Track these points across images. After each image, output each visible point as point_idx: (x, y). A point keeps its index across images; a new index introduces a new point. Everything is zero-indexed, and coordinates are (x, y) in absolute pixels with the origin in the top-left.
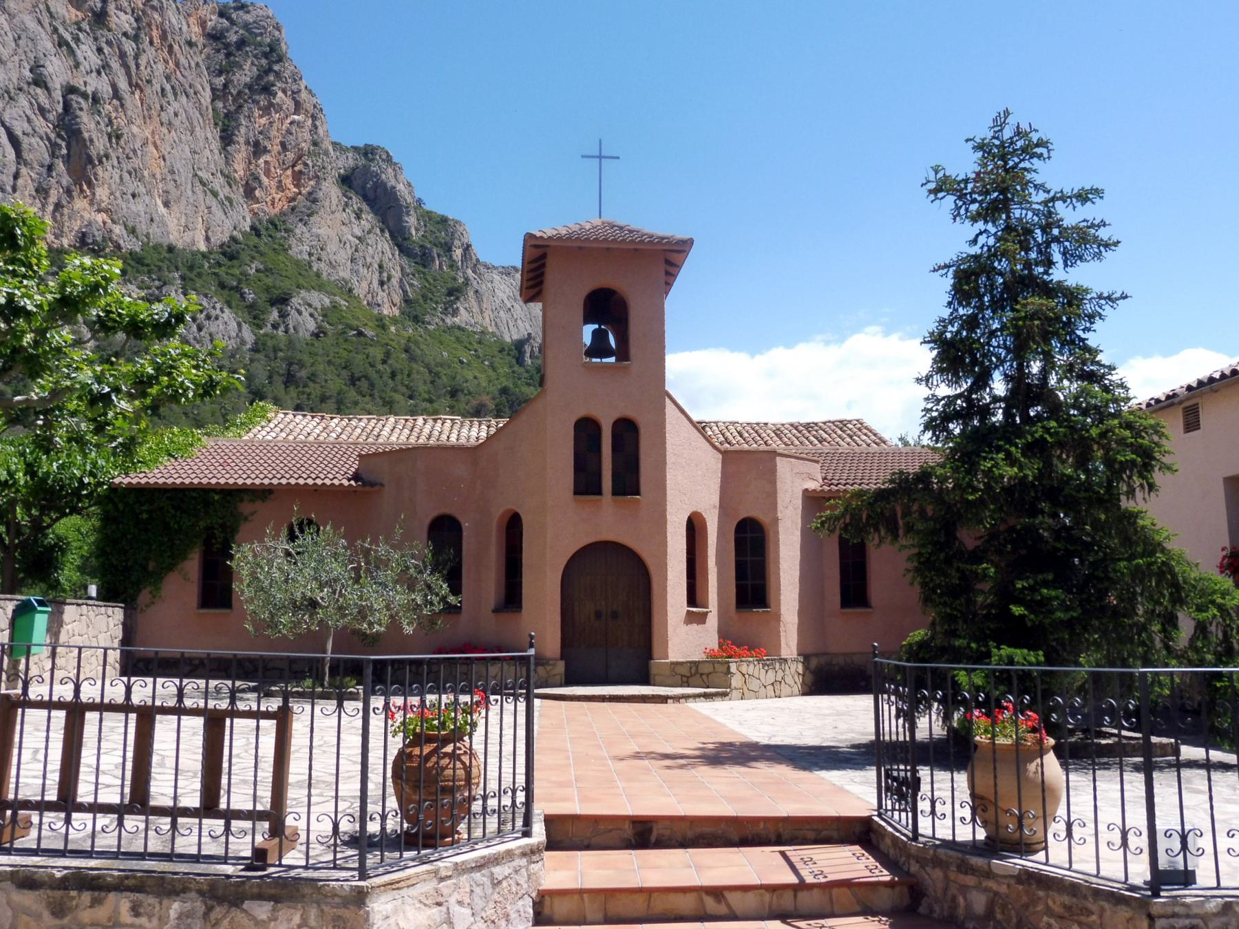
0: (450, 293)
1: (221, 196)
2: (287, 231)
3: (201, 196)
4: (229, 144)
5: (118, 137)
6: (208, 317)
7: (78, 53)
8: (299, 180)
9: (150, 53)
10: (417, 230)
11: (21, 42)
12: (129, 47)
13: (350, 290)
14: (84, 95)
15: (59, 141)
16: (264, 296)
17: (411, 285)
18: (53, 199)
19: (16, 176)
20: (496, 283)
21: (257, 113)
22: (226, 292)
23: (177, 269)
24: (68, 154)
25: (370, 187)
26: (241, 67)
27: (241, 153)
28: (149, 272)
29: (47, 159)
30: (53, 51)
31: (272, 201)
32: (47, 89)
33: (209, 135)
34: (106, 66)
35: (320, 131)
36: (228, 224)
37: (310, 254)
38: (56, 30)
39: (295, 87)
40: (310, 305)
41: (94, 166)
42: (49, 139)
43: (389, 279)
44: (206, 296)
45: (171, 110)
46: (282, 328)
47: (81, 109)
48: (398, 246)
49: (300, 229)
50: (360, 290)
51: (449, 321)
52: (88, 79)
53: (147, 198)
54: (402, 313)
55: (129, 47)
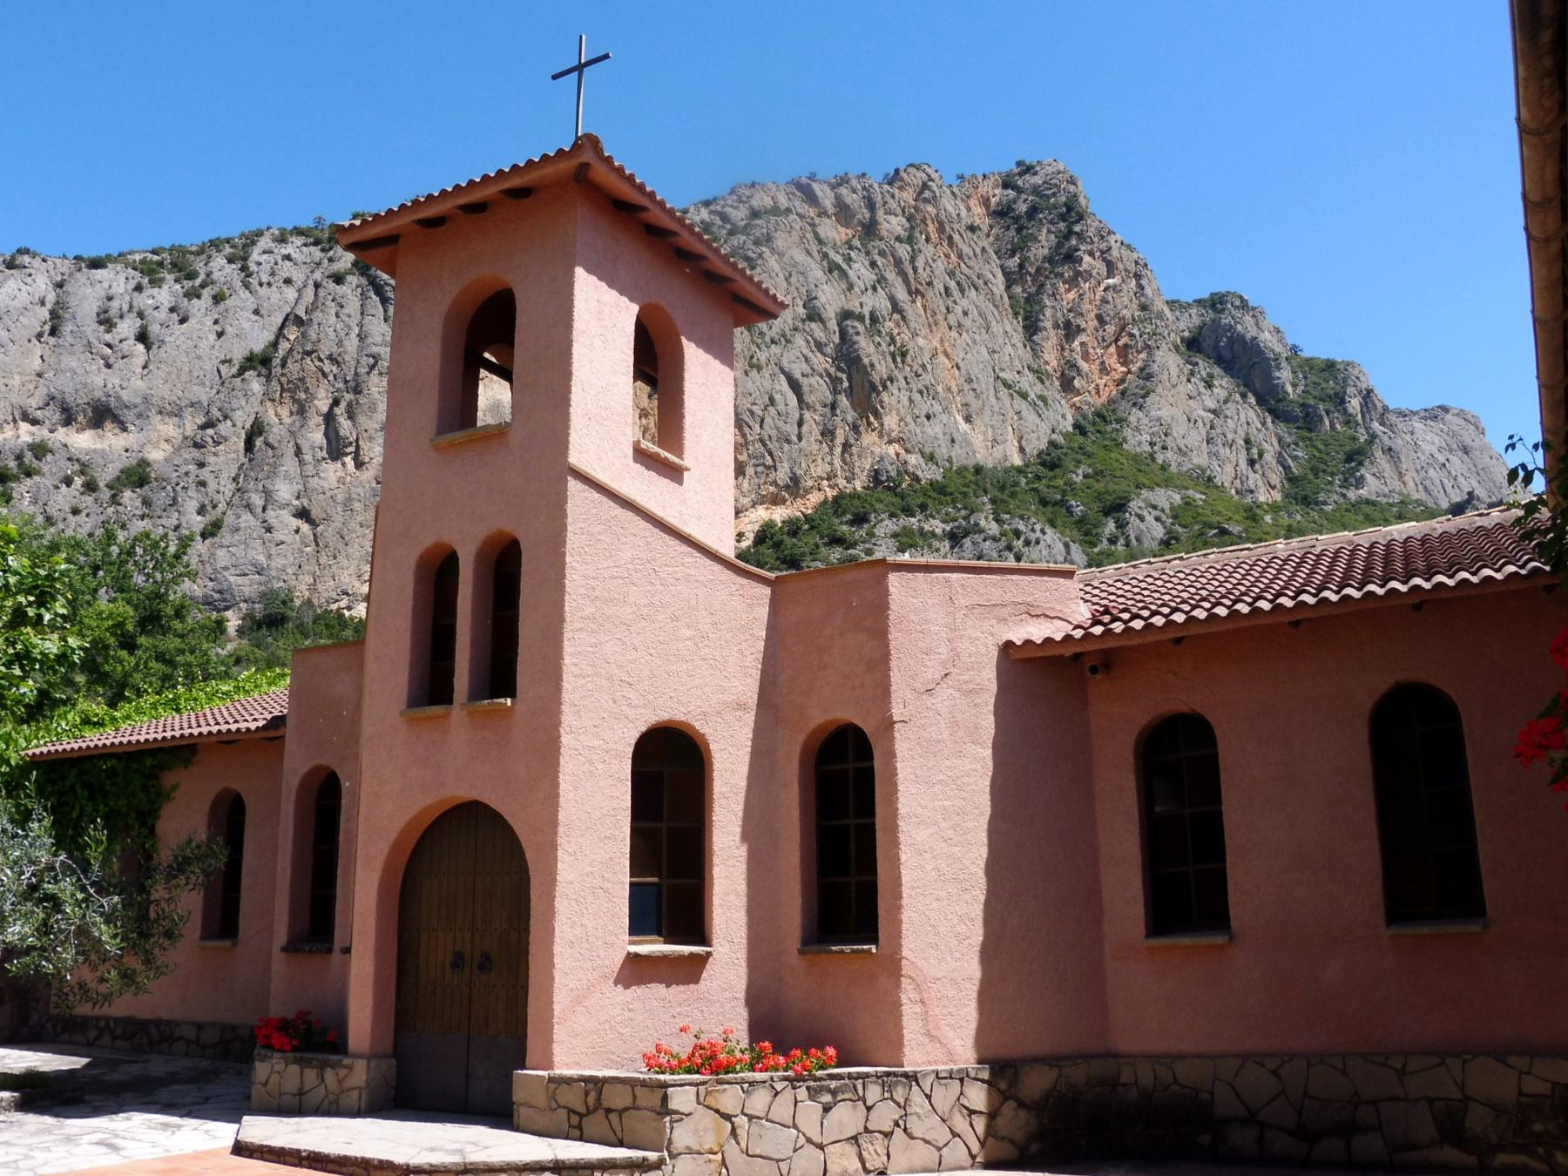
0: (1349, 458)
1: (1032, 396)
2: (1119, 421)
3: (1006, 401)
4: (1035, 333)
5: (904, 355)
6: (1027, 543)
7: (851, 273)
8: (1126, 356)
9: (928, 250)
10: (1294, 385)
11: (792, 280)
12: (903, 251)
13: (1210, 479)
14: (861, 318)
15: (840, 374)
16: (1096, 506)
17: (1295, 458)
18: (840, 440)
19: (800, 423)
20: (1419, 434)
21: (1062, 288)
22: (1050, 508)
23: (986, 492)
24: (850, 387)
25: (1225, 346)
26: (1036, 239)
27: (1050, 340)
28: (954, 501)
29: (829, 397)
30: (824, 278)
31: (1096, 388)
32: (822, 321)
33: (1008, 328)
34: (881, 280)
35: (1148, 291)
36: (1045, 429)
37: (1152, 444)
38: (825, 255)
39: (1103, 246)
40: (1155, 507)
41: (878, 394)
42: (829, 375)
43: (1261, 455)
44: (1022, 517)
45: (958, 310)
46: (1122, 541)
47: (858, 334)
48: (1271, 411)
49: (1135, 415)
50: (1224, 476)
51: (1352, 495)
52: (864, 299)
53: (944, 418)
54: (1286, 496)
55: (903, 251)
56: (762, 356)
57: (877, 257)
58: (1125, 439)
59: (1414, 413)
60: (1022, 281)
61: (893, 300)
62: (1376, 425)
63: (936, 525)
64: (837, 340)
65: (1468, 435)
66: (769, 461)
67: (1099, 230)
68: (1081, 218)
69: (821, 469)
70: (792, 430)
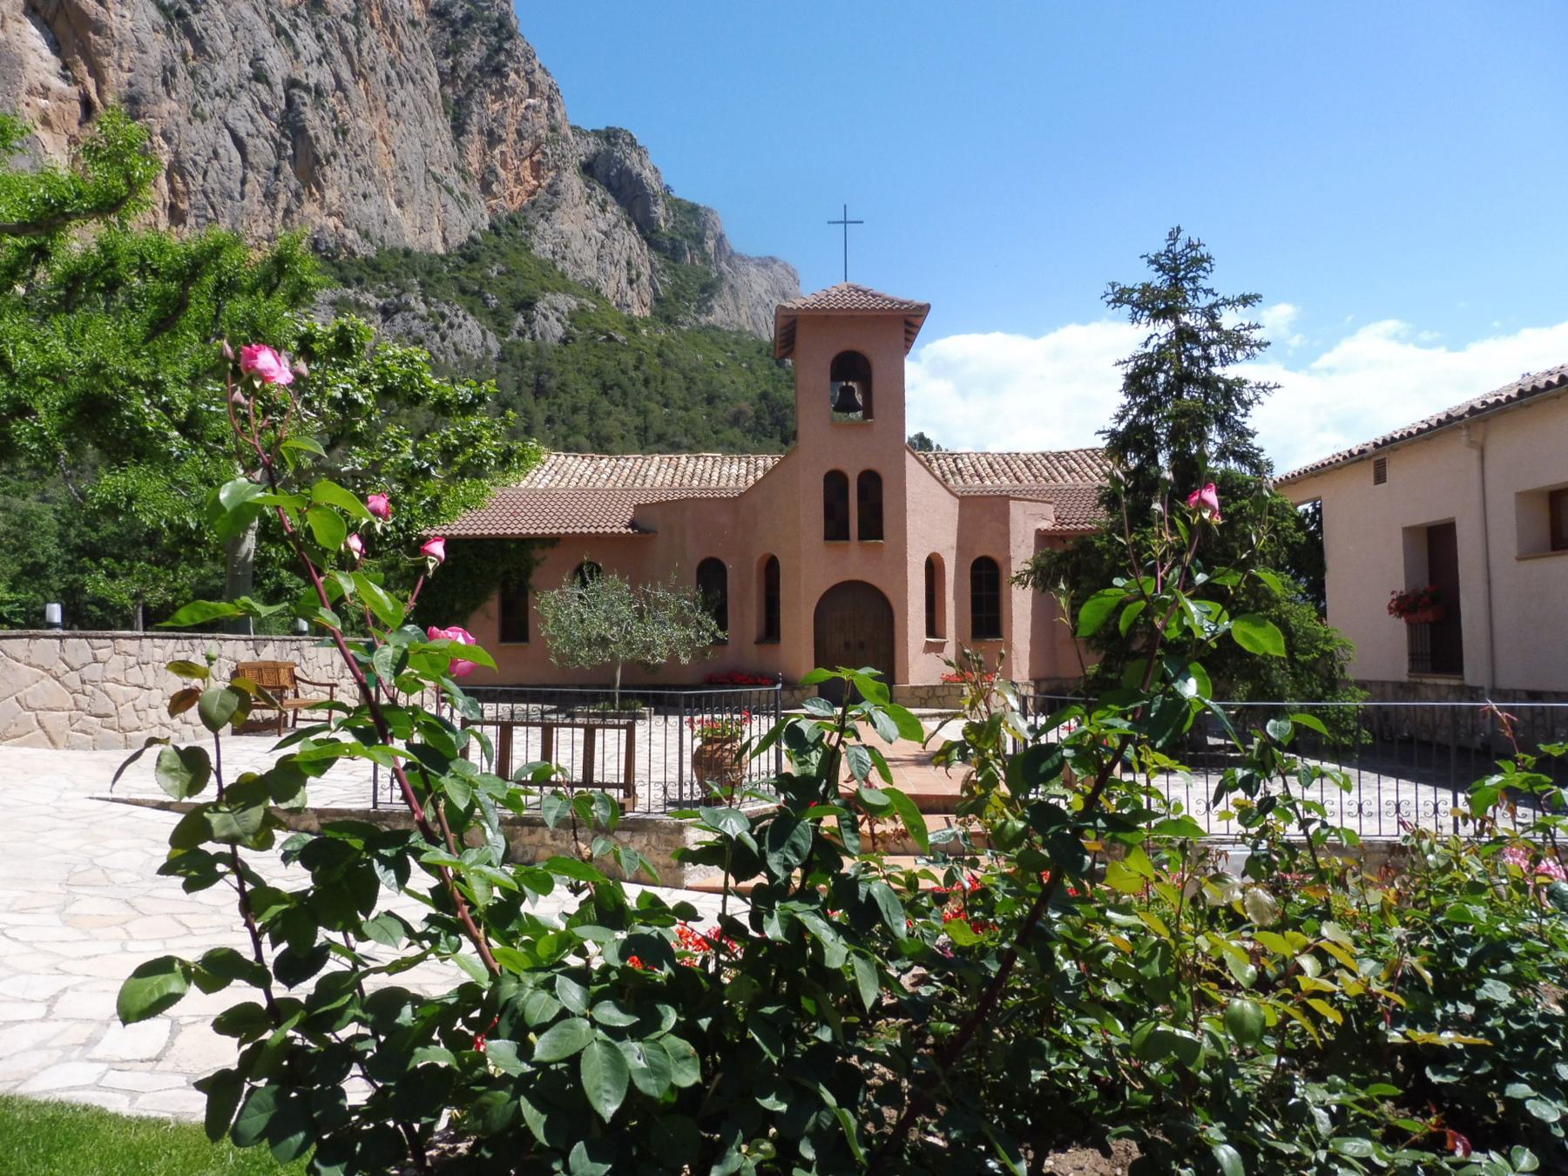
0: (703, 289)
1: (457, 192)
2: (529, 228)
3: (435, 193)
4: (461, 134)
5: (345, 133)
6: (451, 326)
7: (297, 41)
8: (538, 171)
9: (372, 36)
10: (666, 221)
11: (238, 34)
12: (349, 30)
13: (598, 291)
14: (307, 89)
15: (284, 141)
16: (508, 301)
17: (662, 283)
18: (282, 205)
19: (243, 182)
20: (753, 276)
21: (489, 98)
22: (468, 298)
23: (415, 275)
24: (295, 155)
25: (614, 175)
26: (469, 47)
27: (474, 143)
28: (387, 279)
29: (274, 163)
30: (272, 41)
31: (512, 195)
32: (269, 84)
33: (440, 126)
34: (326, 54)
35: (558, 115)
36: (466, 224)
37: (554, 253)
38: (272, 18)
39: (528, 67)
40: (556, 309)
41: (322, 166)
42: (274, 139)
43: (638, 276)
44: (447, 303)
45: (397, 99)
46: (528, 335)
47: (304, 104)
48: (645, 238)
49: (542, 225)
50: (608, 290)
51: (703, 320)
52: (309, 70)
53: (379, 199)
54: (653, 313)
55: (349, 30)
56: (206, 107)
57: (323, 31)
58: (532, 246)
59: (751, 259)
60: (453, 83)
61: (337, 76)
62: (723, 265)
63: (370, 299)
64: (283, 107)
65: (787, 284)
66: (211, 214)
67: (526, 52)
68: (511, 37)
69: (261, 230)
70: (236, 187)
